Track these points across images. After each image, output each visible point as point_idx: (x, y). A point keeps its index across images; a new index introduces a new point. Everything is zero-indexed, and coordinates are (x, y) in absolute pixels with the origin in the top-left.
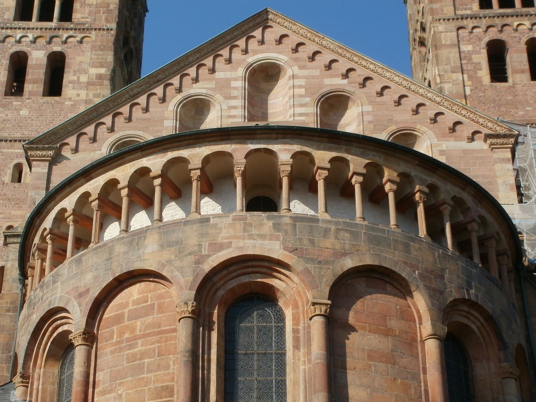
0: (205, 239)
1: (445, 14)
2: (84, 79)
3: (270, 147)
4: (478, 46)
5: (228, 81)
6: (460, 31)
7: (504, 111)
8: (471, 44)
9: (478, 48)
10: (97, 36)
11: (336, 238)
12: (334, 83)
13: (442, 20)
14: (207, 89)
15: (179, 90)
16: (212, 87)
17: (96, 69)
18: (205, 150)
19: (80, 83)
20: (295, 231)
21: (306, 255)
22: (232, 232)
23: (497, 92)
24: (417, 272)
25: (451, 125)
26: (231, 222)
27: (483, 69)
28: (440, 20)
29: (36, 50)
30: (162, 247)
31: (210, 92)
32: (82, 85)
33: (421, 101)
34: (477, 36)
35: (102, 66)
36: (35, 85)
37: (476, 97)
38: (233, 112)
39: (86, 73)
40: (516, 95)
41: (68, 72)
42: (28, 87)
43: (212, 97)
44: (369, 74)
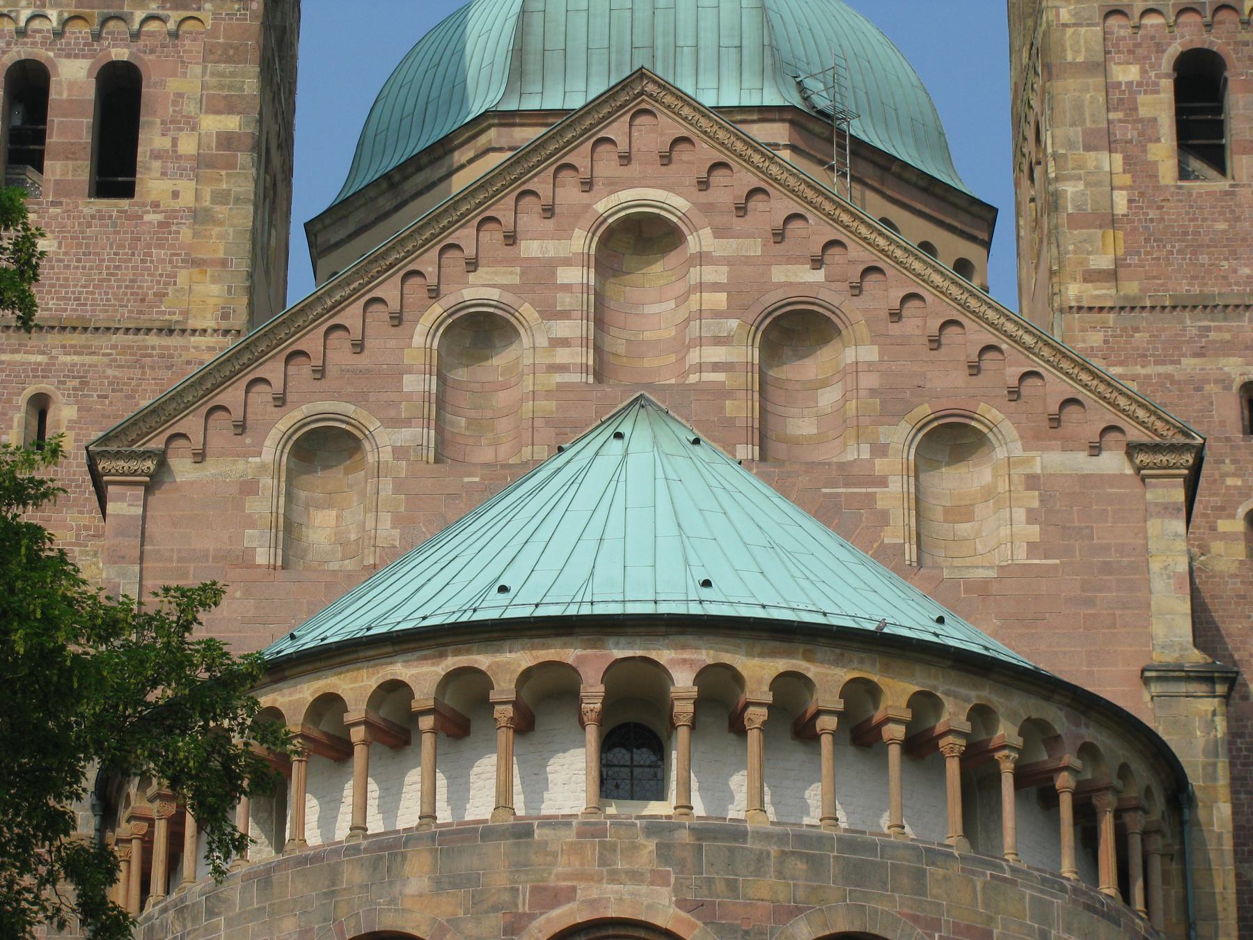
0: (523, 878)
2: (188, 145)
3: (653, 655)
4: (1152, 67)
5: (550, 266)
6: (1113, 21)
7: (1202, 265)
9: (1152, 74)
11: (780, 874)
12: (792, 279)
16: (514, 282)
17: (218, 117)
19: (179, 157)
21: (721, 917)
22: (577, 864)
23: (1191, 207)
26: (575, 839)
27: (1163, 140)
29: (68, 56)
30: (442, 883)
31: (508, 298)
32: (183, 163)
34: (1153, 38)
35: (230, 110)
36: (70, 163)
38: (562, 356)
39: (193, 129)
40: (1238, 219)
41: (151, 124)
42: (54, 168)
43: (512, 311)
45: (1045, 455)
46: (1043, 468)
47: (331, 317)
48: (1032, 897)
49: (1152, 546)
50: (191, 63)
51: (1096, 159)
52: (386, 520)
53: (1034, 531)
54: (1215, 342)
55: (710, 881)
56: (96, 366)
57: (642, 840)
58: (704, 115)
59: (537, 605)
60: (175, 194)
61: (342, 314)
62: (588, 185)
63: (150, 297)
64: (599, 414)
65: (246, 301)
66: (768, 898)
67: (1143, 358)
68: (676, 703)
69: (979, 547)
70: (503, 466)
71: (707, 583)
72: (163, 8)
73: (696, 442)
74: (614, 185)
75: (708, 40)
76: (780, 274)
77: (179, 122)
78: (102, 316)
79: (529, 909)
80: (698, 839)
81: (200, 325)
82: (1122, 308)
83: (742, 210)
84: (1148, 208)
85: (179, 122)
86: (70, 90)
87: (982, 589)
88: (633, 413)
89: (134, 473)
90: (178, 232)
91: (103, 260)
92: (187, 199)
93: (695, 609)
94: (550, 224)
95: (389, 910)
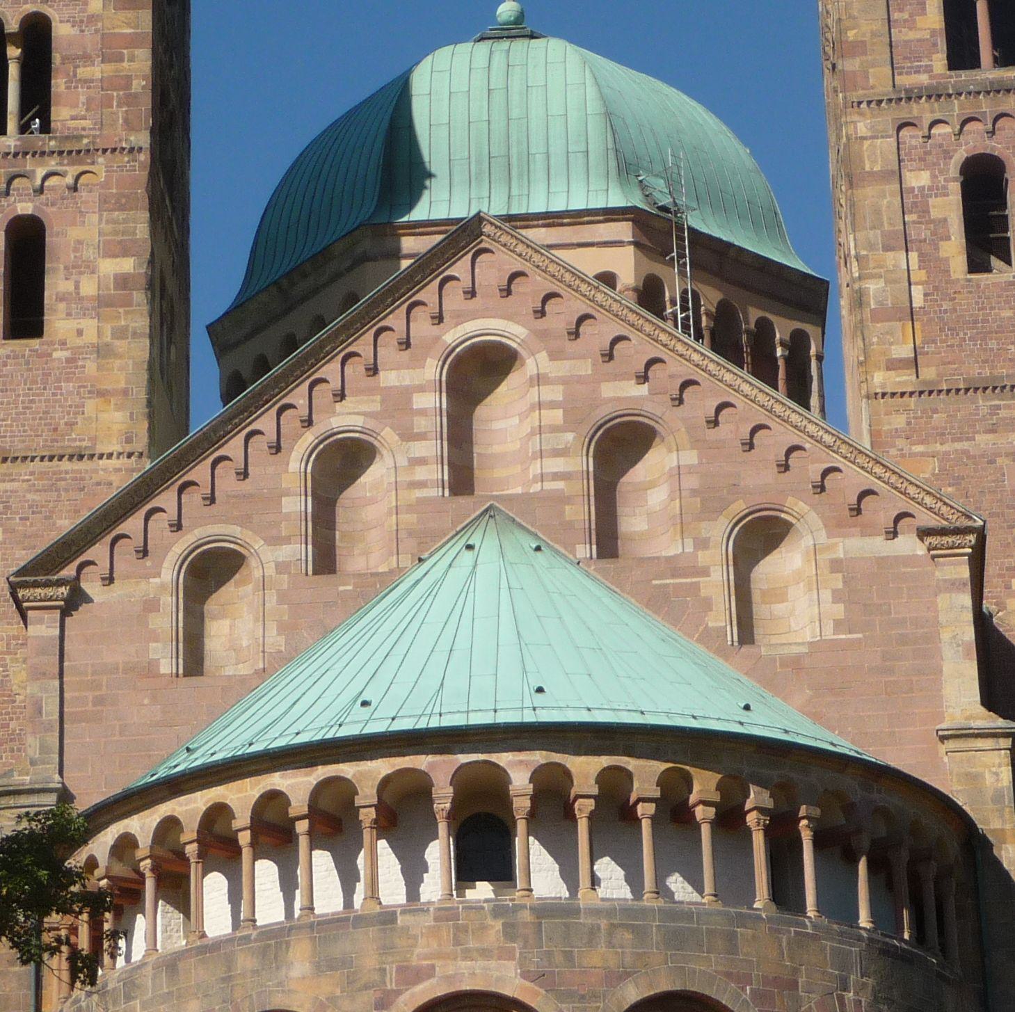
0: (390, 959)
1: (872, 88)
2: (89, 287)
3: (493, 758)
4: (941, 172)
5: (406, 393)
6: (904, 132)
7: (992, 350)
8: (926, 168)
9: (941, 179)
10: (109, 170)
11: (610, 945)
13: (864, 105)
15: (309, 422)
16: (375, 409)
18: (382, 767)
19: (81, 299)
20: (541, 939)
23: (980, 297)
24: (748, 988)
25: (853, 500)
26: (433, 923)
27: (953, 238)
28: (860, 103)
30: (325, 965)
31: (371, 424)
32: (87, 304)
33: (796, 441)
34: (941, 146)
35: (125, 253)
37: (935, 312)
38: (421, 474)
39: (93, 272)
41: (55, 270)
43: (375, 435)
44: (692, 372)
45: (847, 541)
46: (845, 552)
48: (832, 948)
49: (942, 618)
50: (87, 212)
51: (894, 259)
52: (272, 630)
53: (839, 610)
54: (1006, 418)
55: (549, 953)
56: (16, 492)
57: (490, 921)
58: (536, 251)
59: (393, 719)
60: (80, 333)
62: (439, 318)
63: (62, 426)
64: (454, 524)
65: (146, 425)
66: (600, 965)
67: (941, 435)
68: (514, 799)
69: (793, 625)
70: (372, 574)
71: (540, 690)
72: (61, 164)
73: (538, 549)
74: (460, 318)
75: (557, 147)
76: (609, 390)
77: (80, 267)
78: (21, 446)
79: (396, 985)
80: (538, 918)
81: (107, 450)
82: (921, 393)
83: (575, 334)
84: (941, 300)
85: (80, 267)
87: (795, 664)
88: (483, 524)
89: (50, 599)
90: (84, 367)
91: (19, 395)
92: (90, 337)
93: (529, 717)
95: (278, 991)
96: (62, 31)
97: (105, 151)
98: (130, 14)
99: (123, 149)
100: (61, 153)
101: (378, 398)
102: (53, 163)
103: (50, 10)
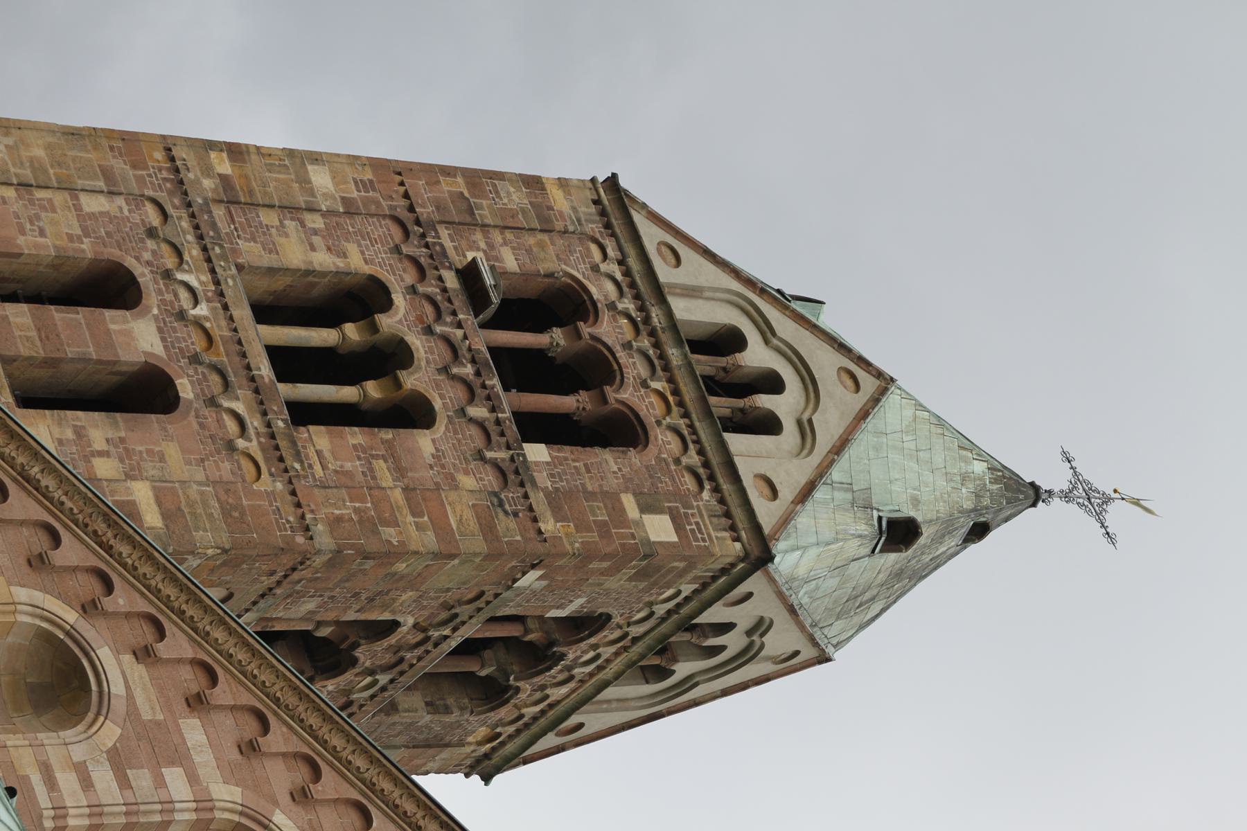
5: (180, 757)
10: (271, 495)
14: (130, 696)
17: (152, 501)
29: (160, 330)
31: (119, 706)
35: (166, 516)
38: (67, 781)
39: (126, 475)
41: (115, 425)
47: (15, 480)
61: (23, 494)
62: (301, 796)
72: (258, 434)
86: (120, 332)
94: (235, 755)
96: (424, 442)
97: (293, 493)
98: (473, 525)
99: (303, 517)
100: (273, 436)
101: (160, 717)
102: (256, 424)
103: (443, 429)
